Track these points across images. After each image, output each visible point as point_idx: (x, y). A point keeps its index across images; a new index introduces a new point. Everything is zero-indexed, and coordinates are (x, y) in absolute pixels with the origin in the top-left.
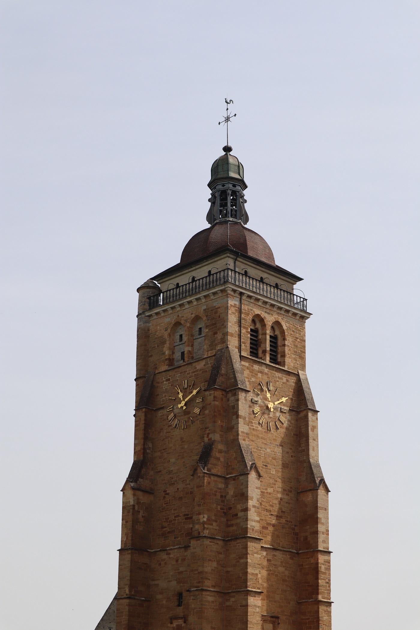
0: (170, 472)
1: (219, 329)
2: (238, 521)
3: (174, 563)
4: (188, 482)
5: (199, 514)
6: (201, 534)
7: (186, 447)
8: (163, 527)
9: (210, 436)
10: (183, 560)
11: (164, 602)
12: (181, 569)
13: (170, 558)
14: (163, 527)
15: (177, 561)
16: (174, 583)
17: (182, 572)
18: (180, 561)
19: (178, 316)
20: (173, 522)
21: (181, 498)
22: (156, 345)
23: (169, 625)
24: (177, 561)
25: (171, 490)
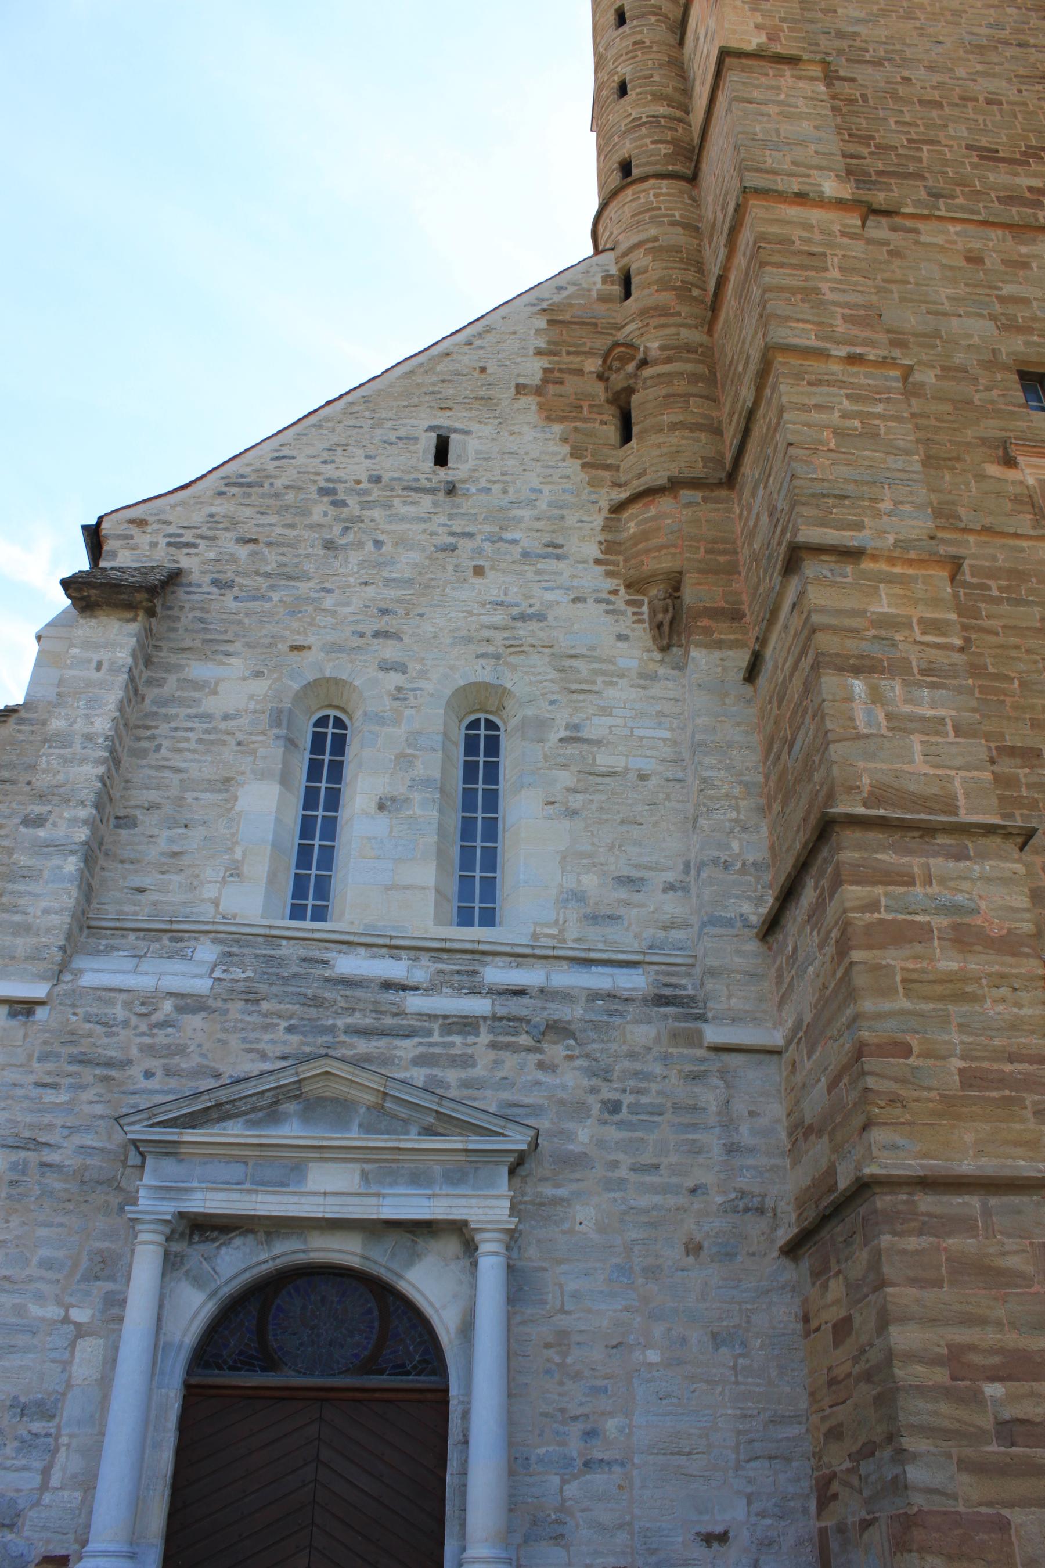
23: (993, 470)
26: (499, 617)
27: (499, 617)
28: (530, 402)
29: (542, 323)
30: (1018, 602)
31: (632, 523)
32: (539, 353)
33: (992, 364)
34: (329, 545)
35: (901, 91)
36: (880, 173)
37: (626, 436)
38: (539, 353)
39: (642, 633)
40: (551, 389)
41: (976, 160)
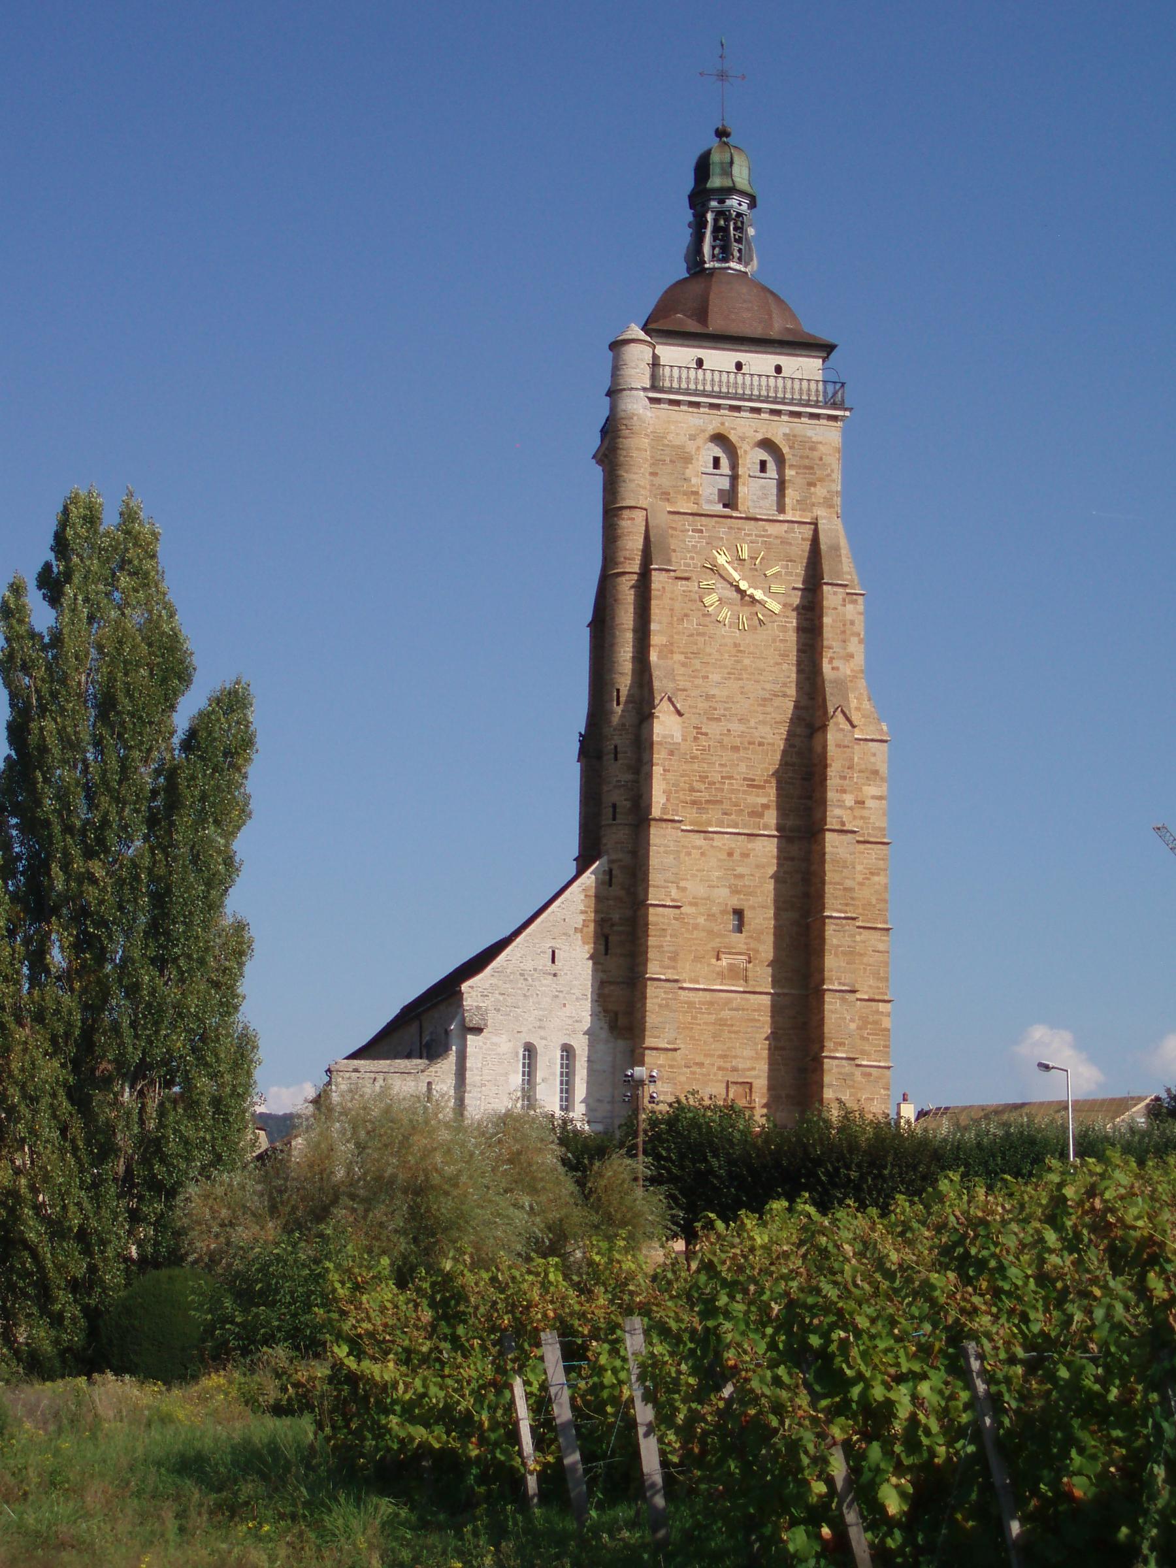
0: (709, 697)
1: (821, 480)
2: (866, 813)
3: (724, 856)
4: (752, 723)
5: (844, 791)
6: (848, 827)
7: (747, 661)
8: (692, 790)
9: (836, 663)
10: (745, 855)
11: (701, 920)
12: (740, 870)
13: (712, 846)
14: (692, 790)
15: (730, 854)
16: (724, 892)
17: (741, 876)
18: (736, 856)
19: (723, 424)
20: (718, 786)
21: (735, 749)
22: (668, 459)
23: (714, 961)
24: (730, 854)
25: (713, 729)
26: (570, 1022)
27: (570, 1022)
28: (579, 935)
29: (583, 897)
30: (709, 1014)
31: (606, 991)
32: (582, 912)
33: (724, 912)
34: (525, 995)
35: (726, 740)
36: (708, 802)
37: (606, 954)
38: (582, 912)
39: (606, 1026)
40: (585, 929)
41: (745, 788)
